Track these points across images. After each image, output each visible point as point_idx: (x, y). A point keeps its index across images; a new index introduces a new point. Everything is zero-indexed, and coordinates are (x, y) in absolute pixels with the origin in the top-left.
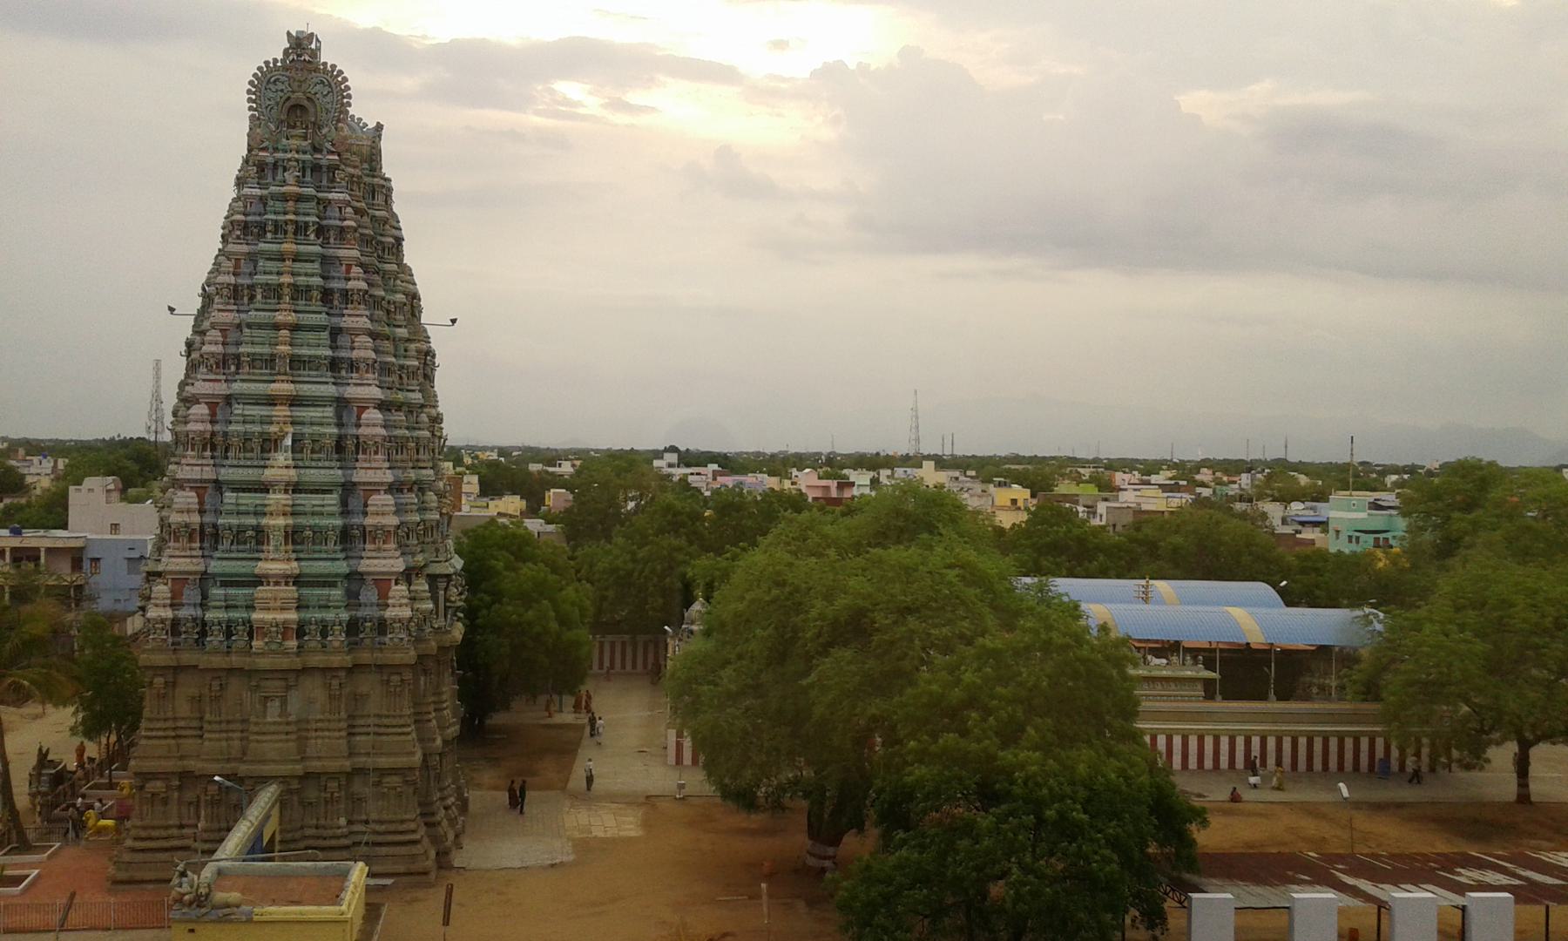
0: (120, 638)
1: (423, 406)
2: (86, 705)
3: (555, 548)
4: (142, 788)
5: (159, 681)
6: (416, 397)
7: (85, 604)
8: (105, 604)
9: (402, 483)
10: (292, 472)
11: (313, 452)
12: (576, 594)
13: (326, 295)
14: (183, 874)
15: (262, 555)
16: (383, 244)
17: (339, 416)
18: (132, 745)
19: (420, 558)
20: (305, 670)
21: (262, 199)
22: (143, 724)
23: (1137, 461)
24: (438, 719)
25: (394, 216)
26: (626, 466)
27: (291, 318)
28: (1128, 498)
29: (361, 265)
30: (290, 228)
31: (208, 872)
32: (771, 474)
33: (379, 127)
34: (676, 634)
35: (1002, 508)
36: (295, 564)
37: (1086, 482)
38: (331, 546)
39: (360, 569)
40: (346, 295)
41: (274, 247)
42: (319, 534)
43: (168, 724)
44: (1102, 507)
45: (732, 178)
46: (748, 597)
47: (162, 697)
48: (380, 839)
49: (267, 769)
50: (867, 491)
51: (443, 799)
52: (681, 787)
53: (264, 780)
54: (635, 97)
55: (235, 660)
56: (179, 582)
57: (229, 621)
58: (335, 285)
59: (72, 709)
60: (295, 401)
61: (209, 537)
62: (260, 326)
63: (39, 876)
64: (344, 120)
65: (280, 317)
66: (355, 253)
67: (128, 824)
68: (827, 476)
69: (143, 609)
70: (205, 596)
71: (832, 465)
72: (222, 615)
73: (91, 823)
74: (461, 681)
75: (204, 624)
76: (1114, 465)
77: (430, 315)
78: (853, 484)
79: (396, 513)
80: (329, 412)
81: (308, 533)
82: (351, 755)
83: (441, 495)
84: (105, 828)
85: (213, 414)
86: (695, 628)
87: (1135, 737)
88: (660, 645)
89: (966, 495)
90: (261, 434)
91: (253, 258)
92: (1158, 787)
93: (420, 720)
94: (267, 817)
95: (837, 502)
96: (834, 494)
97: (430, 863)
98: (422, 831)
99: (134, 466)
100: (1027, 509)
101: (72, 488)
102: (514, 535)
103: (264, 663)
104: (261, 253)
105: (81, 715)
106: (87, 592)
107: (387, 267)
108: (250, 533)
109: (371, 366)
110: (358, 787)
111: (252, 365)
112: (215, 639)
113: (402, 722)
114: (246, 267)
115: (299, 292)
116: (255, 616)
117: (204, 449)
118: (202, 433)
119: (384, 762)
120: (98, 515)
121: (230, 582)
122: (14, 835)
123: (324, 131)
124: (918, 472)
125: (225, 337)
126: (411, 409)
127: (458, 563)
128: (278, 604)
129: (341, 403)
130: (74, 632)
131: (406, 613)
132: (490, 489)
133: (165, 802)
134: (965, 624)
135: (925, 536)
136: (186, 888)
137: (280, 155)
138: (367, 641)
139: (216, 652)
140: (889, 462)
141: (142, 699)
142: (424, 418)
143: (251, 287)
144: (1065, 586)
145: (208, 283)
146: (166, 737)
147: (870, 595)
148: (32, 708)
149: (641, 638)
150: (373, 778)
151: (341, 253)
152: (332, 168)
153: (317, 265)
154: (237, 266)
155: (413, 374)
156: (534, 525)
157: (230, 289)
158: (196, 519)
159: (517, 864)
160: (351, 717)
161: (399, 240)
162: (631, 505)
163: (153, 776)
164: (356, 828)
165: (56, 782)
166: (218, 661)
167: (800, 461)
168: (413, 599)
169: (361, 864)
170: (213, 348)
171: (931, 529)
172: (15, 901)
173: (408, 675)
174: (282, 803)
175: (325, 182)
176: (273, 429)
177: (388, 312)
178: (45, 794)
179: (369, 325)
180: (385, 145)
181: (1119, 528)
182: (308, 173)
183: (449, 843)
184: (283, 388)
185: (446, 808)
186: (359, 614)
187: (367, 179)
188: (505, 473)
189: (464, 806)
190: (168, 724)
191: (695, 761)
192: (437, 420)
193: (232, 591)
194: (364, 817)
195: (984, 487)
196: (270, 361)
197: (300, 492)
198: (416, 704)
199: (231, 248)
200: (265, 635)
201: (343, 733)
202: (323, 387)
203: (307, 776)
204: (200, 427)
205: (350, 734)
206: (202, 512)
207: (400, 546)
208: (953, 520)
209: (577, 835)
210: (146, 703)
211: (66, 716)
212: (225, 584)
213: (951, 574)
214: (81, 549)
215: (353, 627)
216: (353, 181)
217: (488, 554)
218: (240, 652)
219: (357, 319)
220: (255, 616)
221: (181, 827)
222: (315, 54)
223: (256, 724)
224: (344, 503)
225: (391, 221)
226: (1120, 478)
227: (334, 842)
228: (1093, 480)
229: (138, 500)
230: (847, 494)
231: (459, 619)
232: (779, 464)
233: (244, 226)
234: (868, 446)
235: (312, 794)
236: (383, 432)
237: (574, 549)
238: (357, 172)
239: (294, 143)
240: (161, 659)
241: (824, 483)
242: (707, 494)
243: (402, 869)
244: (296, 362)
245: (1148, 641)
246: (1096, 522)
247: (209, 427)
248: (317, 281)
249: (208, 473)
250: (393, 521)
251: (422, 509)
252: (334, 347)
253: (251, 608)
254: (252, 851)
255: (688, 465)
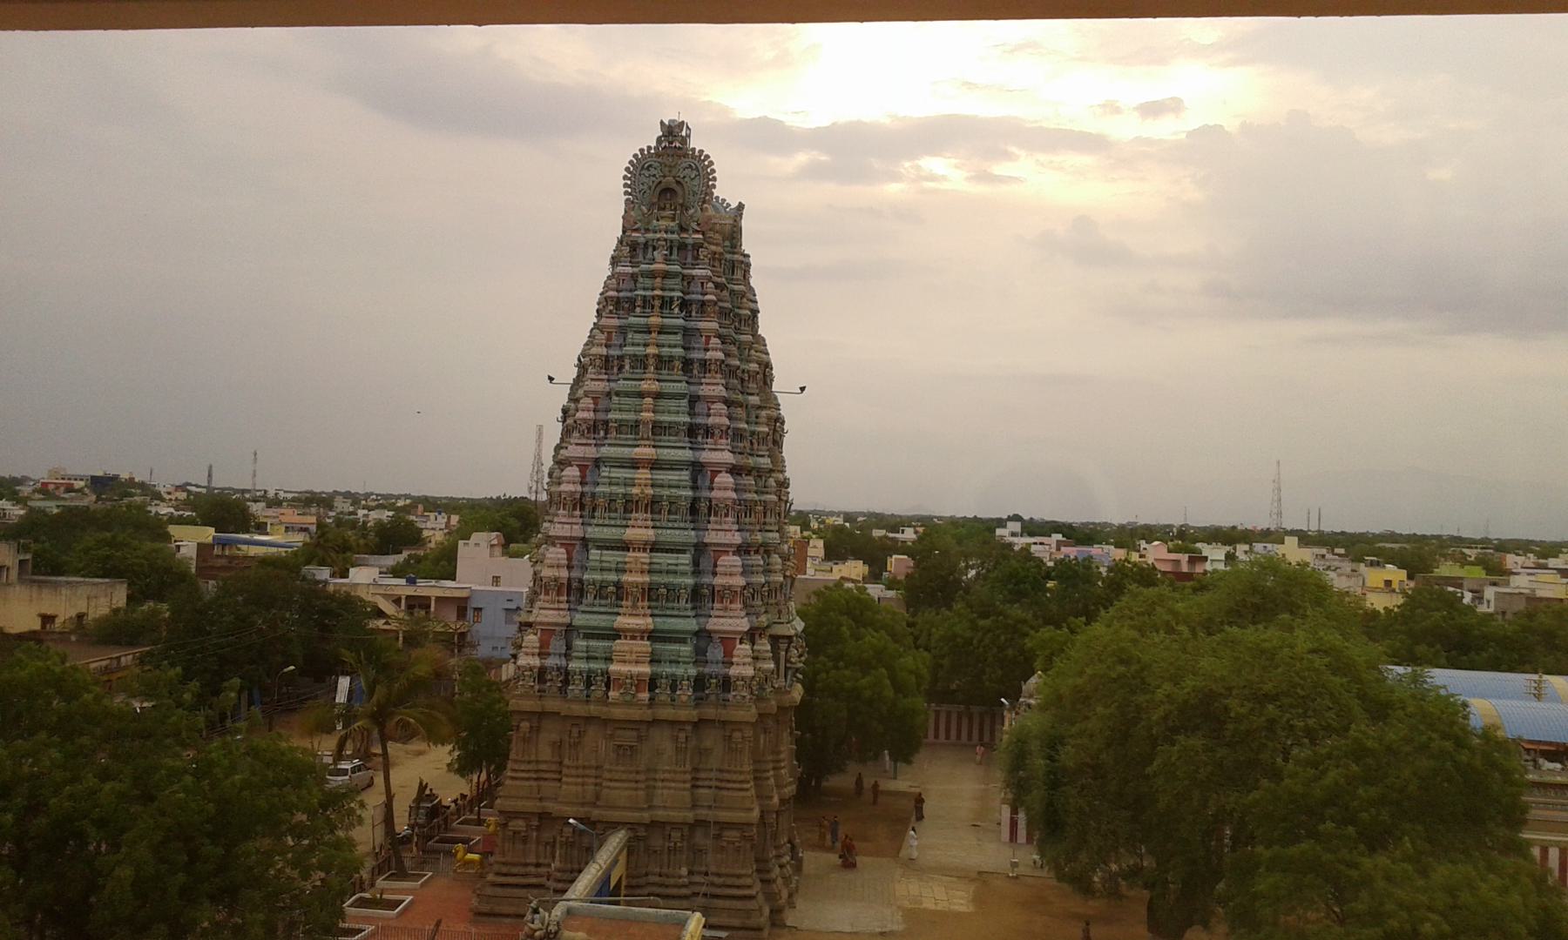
0: (494, 683)
1: (771, 471)
2: (462, 744)
3: (894, 613)
4: (505, 825)
5: (525, 725)
6: (765, 462)
7: (467, 650)
8: (484, 651)
9: (749, 545)
10: (651, 532)
11: (670, 512)
12: (913, 661)
13: (687, 364)
14: (536, 911)
15: (621, 610)
16: (739, 314)
17: (694, 480)
18: (498, 785)
19: (763, 618)
20: (655, 722)
21: (634, 277)
22: (510, 765)
23: (1532, 542)
24: (776, 777)
25: (751, 289)
26: (981, 530)
27: (655, 387)
28: (1521, 583)
29: (719, 336)
30: (657, 303)
31: (558, 911)
32: (1118, 545)
33: (741, 207)
34: (1013, 707)
35: (1374, 590)
36: (650, 620)
37: (1472, 564)
38: (683, 603)
39: (709, 627)
40: (704, 364)
41: (642, 321)
42: (672, 592)
43: (530, 767)
44: (1489, 593)
45: (1085, 244)
46: (1089, 671)
47: (526, 740)
48: (718, 891)
49: (616, 815)
50: (1221, 567)
51: (779, 857)
52: (1015, 865)
53: (614, 826)
54: (999, 169)
55: (593, 709)
56: (547, 632)
57: (590, 671)
58: (696, 355)
59: (450, 747)
60: (655, 465)
61: (575, 591)
62: (627, 394)
63: (411, 902)
64: (709, 202)
65: (645, 386)
66: (715, 325)
67: (491, 859)
68: (1177, 550)
69: (515, 657)
70: (569, 647)
71: (1184, 538)
72: (583, 665)
73: (459, 855)
74: (798, 742)
75: (567, 673)
76: (1504, 547)
77: (781, 383)
78: (1206, 558)
79: (742, 574)
80: (685, 475)
81: (664, 591)
82: (694, 806)
83: (785, 558)
84: (472, 861)
85: (583, 476)
86: (1032, 701)
87: (1521, 849)
88: (996, 717)
89: (1332, 575)
90: (625, 495)
91: (623, 330)
92: (1545, 909)
93: (758, 779)
94: (615, 861)
95: (1188, 577)
96: (1185, 568)
97: (763, 920)
98: (758, 886)
99: (514, 523)
100: (1403, 592)
101: (461, 543)
102: (859, 600)
103: (618, 713)
104: (630, 326)
105: (457, 753)
106: (469, 638)
107: (743, 338)
108: (611, 589)
109: (725, 432)
110: (700, 838)
111: (618, 431)
112: (576, 688)
113: (742, 777)
114: (616, 341)
115: (662, 362)
116: (613, 667)
117: (574, 509)
118: (573, 493)
119: (725, 816)
120: (483, 568)
121: (592, 634)
122: (393, 864)
123: (691, 211)
124: (1279, 549)
125: (596, 404)
126: (758, 473)
127: (799, 625)
128: (634, 657)
129: (697, 468)
130: (456, 676)
131: (749, 671)
132: (834, 553)
133: (525, 840)
134: (1331, 714)
135: (1286, 616)
136: (537, 925)
137: (650, 235)
138: (713, 697)
139: (576, 700)
140: (1248, 537)
141: (510, 742)
142: (772, 482)
143: (621, 358)
144: (1445, 679)
145: (584, 354)
146: (528, 779)
147: (1223, 678)
148: (417, 745)
149: (975, 709)
150: (713, 831)
151: (701, 325)
152: (697, 247)
153: (679, 337)
154: (609, 339)
155: (763, 439)
156: (875, 590)
157: (601, 361)
158: (564, 573)
159: (848, 929)
160: (696, 770)
161: (755, 312)
162: (972, 573)
163: (515, 815)
164: (697, 879)
165: (431, 812)
166: (578, 709)
167: (1149, 533)
168: (756, 658)
169: (698, 914)
170: (585, 415)
171: (1293, 609)
172: (393, 923)
173: (749, 733)
174: (630, 848)
175: (689, 260)
176: (635, 491)
177: (742, 380)
178: (421, 826)
179: (724, 393)
180: (746, 224)
181: (1509, 616)
182: (675, 251)
183: (782, 902)
184: (645, 452)
185: (781, 866)
186: (707, 670)
187: (728, 256)
188: (853, 538)
189: (798, 868)
190: (530, 767)
191: (1029, 839)
192: (784, 484)
193: (593, 643)
194: (703, 869)
195: (1354, 566)
196: (635, 426)
197: (658, 551)
198: (755, 762)
199: (604, 321)
200: (620, 686)
201: (688, 785)
202: (680, 452)
203: (654, 825)
204: (571, 488)
205: (694, 786)
206: (570, 567)
207: (746, 606)
208: (1318, 603)
209: (907, 904)
210: (513, 745)
211: (443, 754)
212: (587, 637)
213: (1319, 662)
214: (466, 599)
215: (699, 683)
216: (715, 258)
217: (835, 617)
218: (599, 701)
219: (713, 387)
220: (613, 667)
221: (538, 865)
222: (684, 140)
223: (610, 771)
224: (696, 563)
225: (748, 295)
226: (1511, 560)
227: (674, 891)
228: (1480, 562)
229: (519, 555)
230: (1199, 569)
231: (798, 680)
232: (1129, 536)
233: (615, 303)
234: (1224, 521)
235: (657, 842)
236: (734, 495)
237: (914, 615)
238: (719, 249)
239: (663, 223)
240: (528, 705)
241: (1173, 556)
242: (1051, 564)
243: (736, 922)
244: (658, 428)
245: (1540, 742)
246: (1482, 609)
247: (579, 488)
248: (679, 351)
249: (577, 531)
250: (740, 581)
251: (767, 571)
252: (692, 414)
253: (609, 660)
254: (600, 893)
255: (1031, 535)
